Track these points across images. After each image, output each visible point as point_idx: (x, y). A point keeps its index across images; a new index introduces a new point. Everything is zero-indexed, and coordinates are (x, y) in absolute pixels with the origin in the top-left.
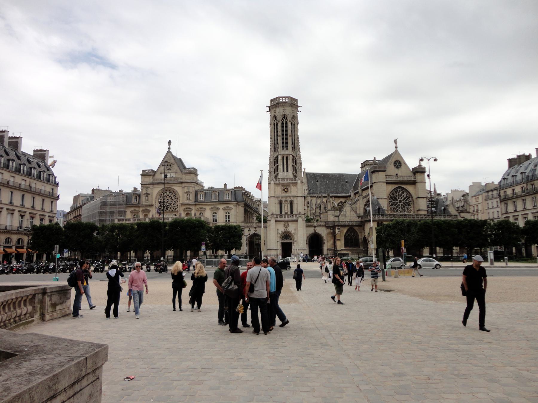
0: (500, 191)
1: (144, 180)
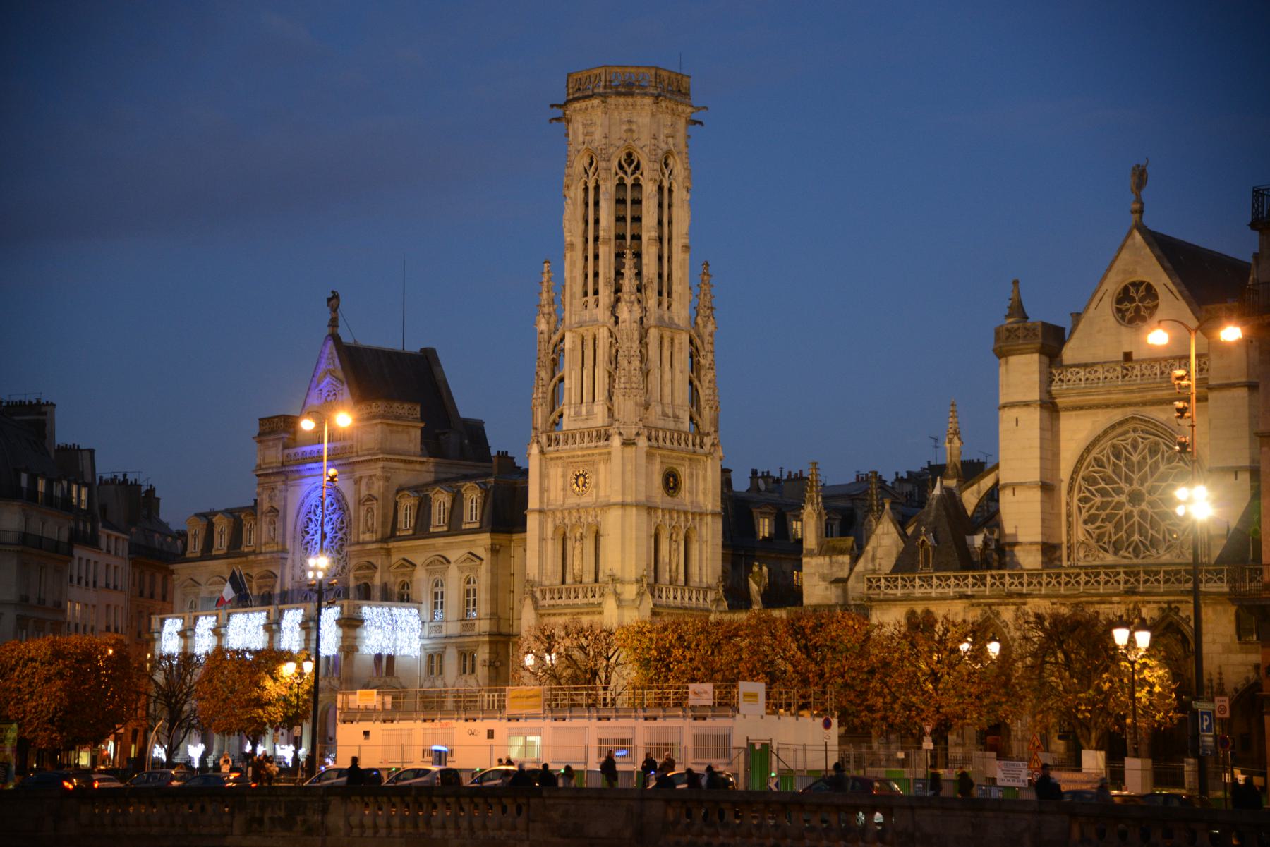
1: (264, 460)
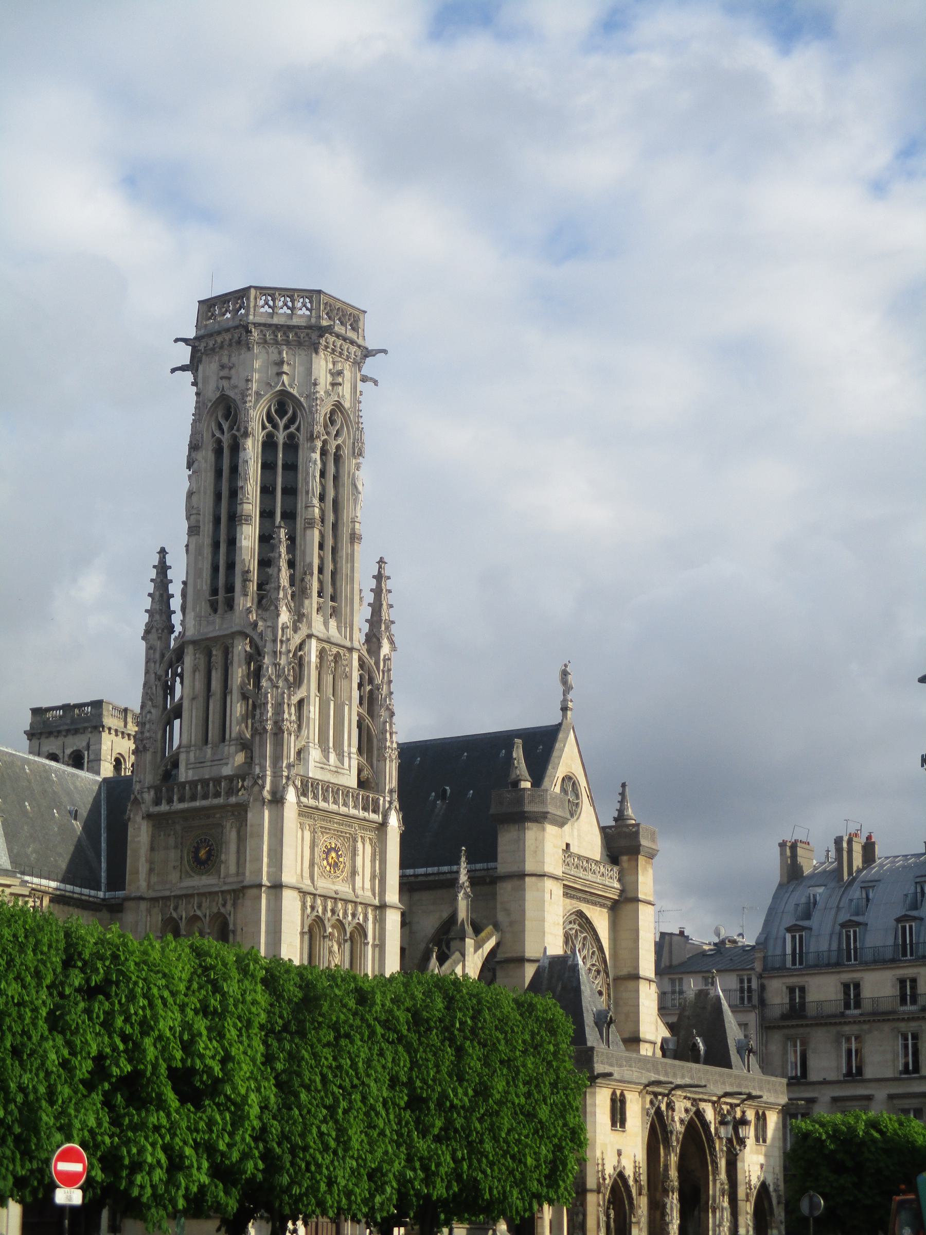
0: (766, 982)
